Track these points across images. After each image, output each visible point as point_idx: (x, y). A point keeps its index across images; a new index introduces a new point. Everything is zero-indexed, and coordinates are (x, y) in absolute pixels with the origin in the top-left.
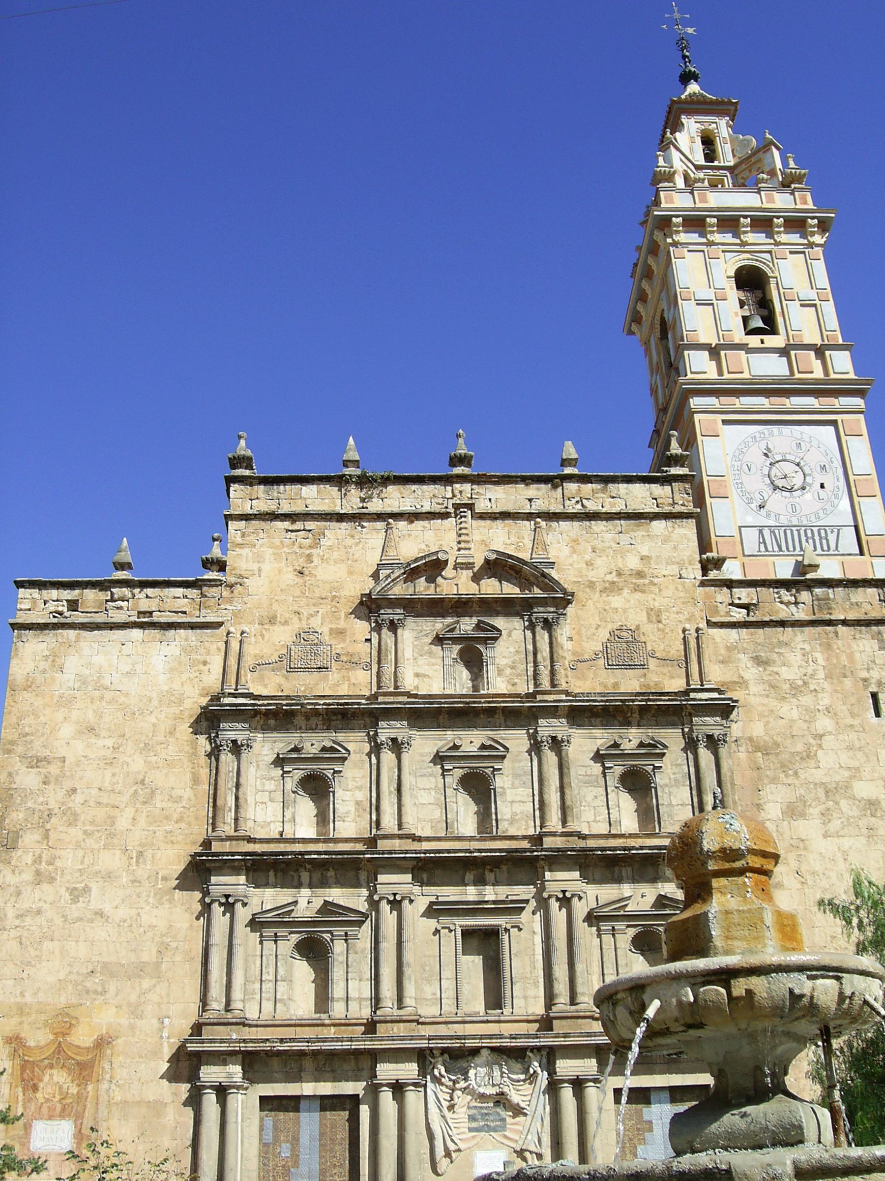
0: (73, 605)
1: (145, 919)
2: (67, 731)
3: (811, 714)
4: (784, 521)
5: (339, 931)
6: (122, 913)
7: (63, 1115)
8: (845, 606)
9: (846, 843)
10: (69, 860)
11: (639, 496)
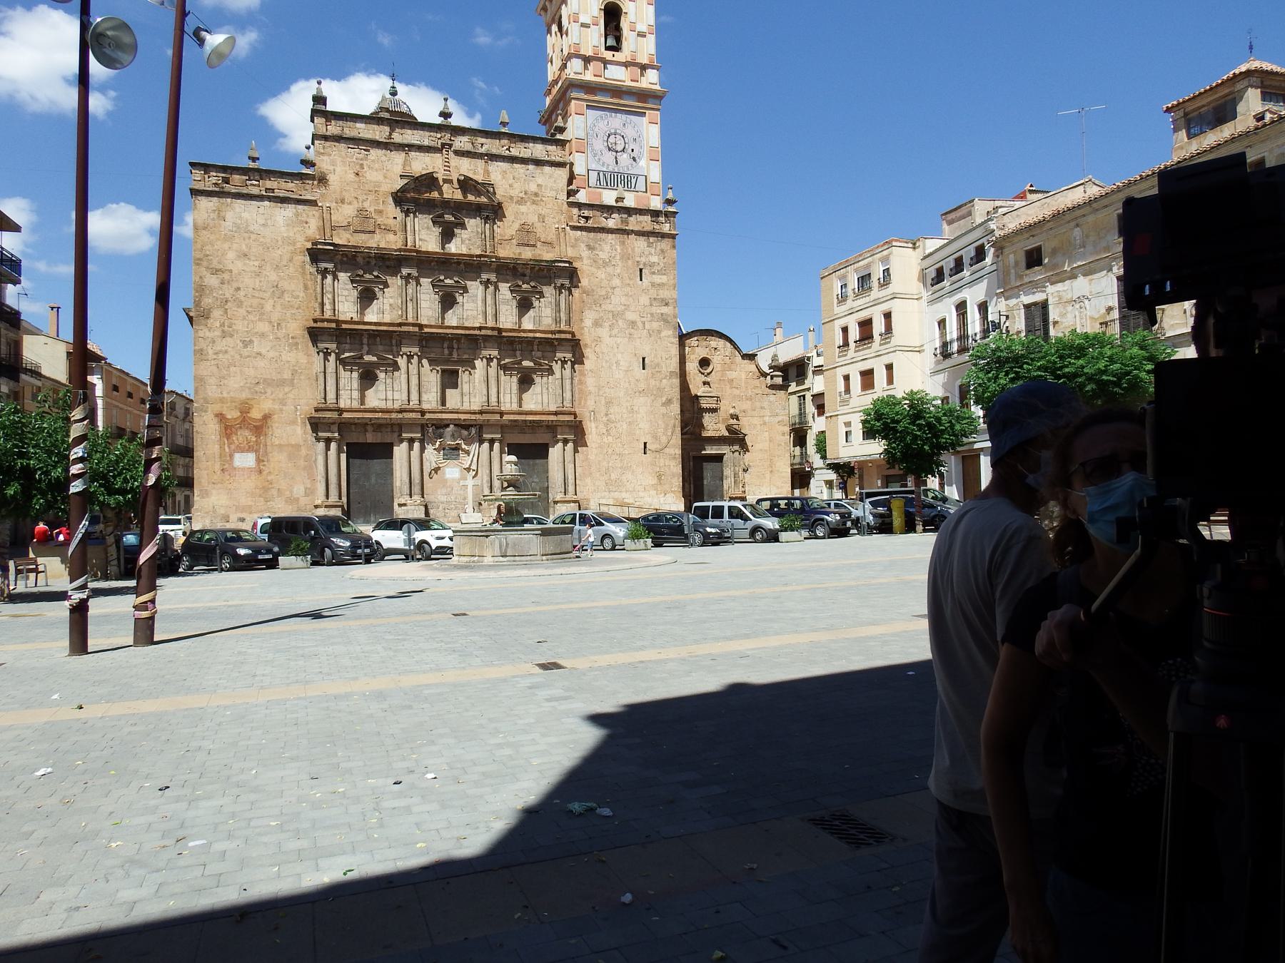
0: (226, 181)
1: (284, 357)
2: (231, 255)
3: (611, 276)
6: (272, 354)
8: (635, 223)
9: (619, 340)
10: (240, 326)
11: (538, 150)
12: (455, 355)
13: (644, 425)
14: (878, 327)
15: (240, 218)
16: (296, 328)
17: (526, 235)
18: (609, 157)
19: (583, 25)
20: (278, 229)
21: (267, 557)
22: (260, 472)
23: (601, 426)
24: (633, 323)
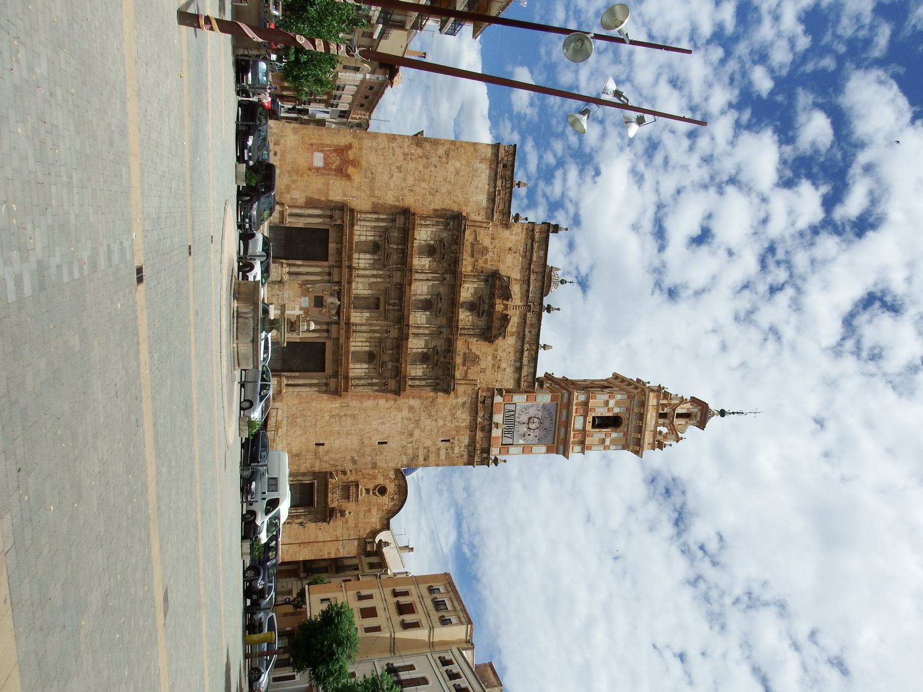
0: (505, 166)
2: (458, 164)
3: (444, 419)
4: (517, 420)
5: (382, 258)
6: (392, 184)
7: (325, 163)
9: (399, 424)
10: (411, 165)
12: (390, 307)
13: (337, 443)
14: (409, 618)
15: (482, 172)
16: (410, 201)
17: (472, 359)
18: (524, 418)
19: (608, 401)
20: (474, 197)
21: (246, 156)
22: (310, 169)
23: (337, 411)
24: (411, 435)
